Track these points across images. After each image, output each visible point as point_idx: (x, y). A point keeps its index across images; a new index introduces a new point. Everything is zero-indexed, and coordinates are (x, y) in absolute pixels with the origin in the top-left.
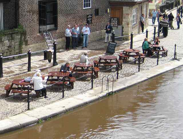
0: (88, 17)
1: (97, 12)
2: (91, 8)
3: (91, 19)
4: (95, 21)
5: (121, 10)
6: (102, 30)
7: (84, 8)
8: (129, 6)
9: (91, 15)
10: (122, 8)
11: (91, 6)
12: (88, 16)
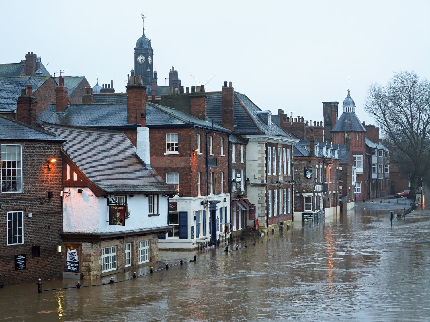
0: (17, 258)
2: (23, 245)
3: (24, 262)
5: (80, 247)
7: (8, 245)
8: (92, 243)
10: (81, 245)
11: (24, 241)
12: (17, 256)
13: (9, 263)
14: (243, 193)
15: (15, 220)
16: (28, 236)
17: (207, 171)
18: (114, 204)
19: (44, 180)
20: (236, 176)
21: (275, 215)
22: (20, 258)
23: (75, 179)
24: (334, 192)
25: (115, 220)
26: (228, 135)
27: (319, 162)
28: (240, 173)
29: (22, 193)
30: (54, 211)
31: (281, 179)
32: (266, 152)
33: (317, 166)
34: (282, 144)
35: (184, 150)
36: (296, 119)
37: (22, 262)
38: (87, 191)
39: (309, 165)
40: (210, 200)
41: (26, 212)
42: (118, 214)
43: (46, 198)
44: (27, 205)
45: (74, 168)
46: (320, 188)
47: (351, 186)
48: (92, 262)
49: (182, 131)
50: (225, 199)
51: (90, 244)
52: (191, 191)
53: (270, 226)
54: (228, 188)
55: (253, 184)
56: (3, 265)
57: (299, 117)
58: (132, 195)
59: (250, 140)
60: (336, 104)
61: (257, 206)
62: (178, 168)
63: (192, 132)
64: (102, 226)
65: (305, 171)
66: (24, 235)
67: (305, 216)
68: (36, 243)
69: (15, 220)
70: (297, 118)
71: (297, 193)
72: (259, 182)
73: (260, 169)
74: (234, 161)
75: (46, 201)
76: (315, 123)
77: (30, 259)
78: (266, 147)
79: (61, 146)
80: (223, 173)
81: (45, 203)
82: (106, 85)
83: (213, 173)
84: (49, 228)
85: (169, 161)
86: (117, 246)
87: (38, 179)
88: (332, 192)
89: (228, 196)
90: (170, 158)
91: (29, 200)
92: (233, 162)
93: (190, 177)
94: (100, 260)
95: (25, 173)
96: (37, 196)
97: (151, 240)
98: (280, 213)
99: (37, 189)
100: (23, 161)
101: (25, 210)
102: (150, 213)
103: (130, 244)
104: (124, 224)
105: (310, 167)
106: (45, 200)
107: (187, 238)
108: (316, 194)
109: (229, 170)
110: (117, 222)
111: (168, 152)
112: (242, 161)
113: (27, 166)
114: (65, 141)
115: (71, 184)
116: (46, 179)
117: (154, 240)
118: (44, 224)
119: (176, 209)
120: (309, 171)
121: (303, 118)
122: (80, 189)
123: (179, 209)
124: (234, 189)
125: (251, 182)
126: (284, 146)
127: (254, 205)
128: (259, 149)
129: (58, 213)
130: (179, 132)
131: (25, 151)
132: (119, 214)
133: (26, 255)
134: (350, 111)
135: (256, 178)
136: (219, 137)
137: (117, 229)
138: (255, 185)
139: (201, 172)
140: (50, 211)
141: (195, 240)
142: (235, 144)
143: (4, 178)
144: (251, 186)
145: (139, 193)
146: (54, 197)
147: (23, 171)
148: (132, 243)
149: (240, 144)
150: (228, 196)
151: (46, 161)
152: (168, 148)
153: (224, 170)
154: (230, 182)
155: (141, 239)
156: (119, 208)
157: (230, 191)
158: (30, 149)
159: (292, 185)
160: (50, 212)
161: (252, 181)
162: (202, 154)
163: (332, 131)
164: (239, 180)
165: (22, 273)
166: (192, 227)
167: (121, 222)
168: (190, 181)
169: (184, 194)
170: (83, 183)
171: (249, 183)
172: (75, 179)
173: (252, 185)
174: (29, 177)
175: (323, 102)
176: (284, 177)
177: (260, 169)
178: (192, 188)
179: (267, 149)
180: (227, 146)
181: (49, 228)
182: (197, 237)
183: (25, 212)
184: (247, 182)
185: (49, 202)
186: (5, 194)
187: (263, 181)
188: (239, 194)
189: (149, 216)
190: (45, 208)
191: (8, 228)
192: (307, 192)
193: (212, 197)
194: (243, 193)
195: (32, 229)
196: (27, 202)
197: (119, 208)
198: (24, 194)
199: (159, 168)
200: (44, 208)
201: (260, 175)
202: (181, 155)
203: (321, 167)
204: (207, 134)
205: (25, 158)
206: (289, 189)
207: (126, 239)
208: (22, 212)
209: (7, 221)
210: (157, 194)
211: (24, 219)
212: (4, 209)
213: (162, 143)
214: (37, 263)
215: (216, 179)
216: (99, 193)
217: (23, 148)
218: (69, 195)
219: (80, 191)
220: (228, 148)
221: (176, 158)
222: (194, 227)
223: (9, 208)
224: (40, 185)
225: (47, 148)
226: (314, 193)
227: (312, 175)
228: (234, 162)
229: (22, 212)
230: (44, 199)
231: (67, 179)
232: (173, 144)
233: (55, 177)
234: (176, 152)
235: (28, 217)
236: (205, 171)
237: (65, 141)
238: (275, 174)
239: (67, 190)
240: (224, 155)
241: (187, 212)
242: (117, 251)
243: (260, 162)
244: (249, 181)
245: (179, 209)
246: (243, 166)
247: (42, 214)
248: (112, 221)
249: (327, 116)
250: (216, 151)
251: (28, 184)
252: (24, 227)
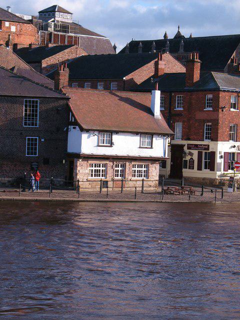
15: (32, 143)
38: (77, 127)
45: (73, 115)
58: (117, 132)
69: (32, 143)
84: (57, 148)
115: (72, 124)
183: (39, 138)
202: (213, 111)
219: (74, 128)
230: (53, 131)
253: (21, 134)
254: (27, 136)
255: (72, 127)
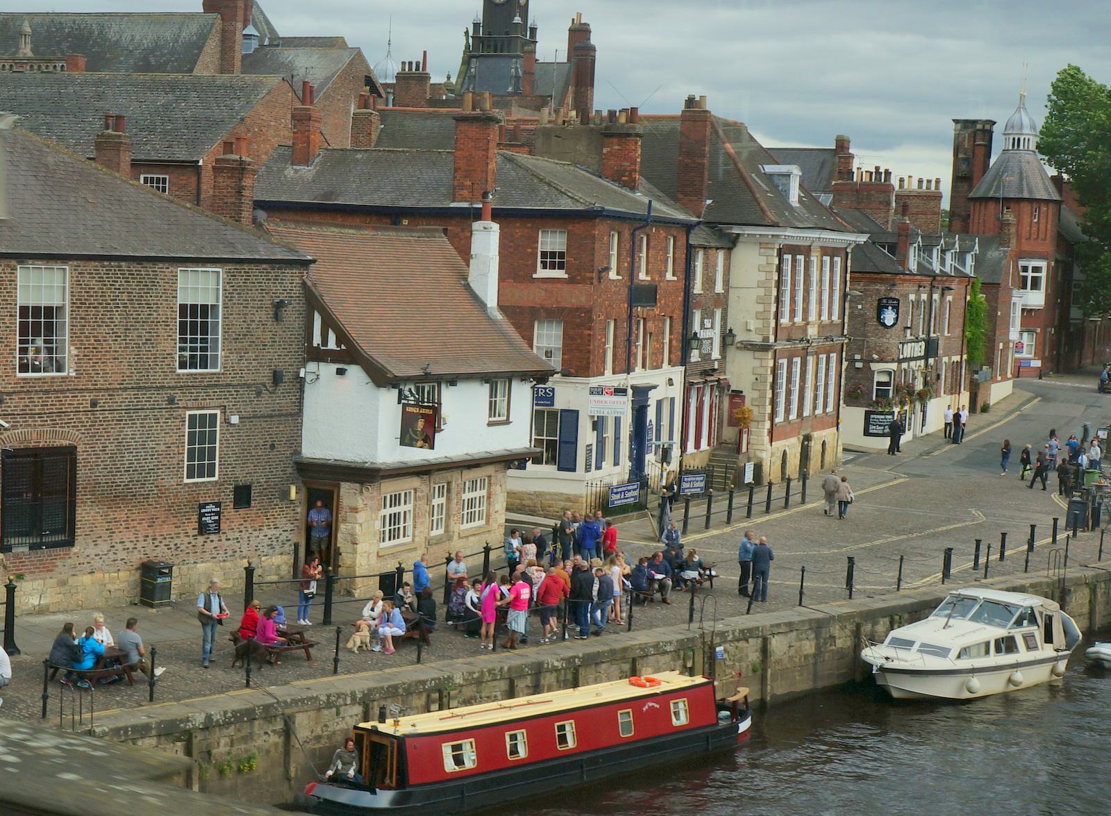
0: (203, 511)
1: (243, 496)
2: (216, 482)
3: (217, 518)
4: (235, 525)
6: (263, 558)
7: (186, 481)
8: (362, 483)
9: (218, 505)
13: (186, 519)
14: (716, 363)
15: (202, 430)
16: (228, 464)
17: (630, 317)
18: (412, 403)
19: (266, 345)
20: (702, 324)
21: (793, 416)
22: (209, 510)
23: (332, 345)
24: (956, 358)
25: (414, 436)
26: (688, 228)
27: (920, 286)
28: (711, 316)
29: (219, 374)
30: (284, 412)
31: (812, 332)
32: (779, 269)
33: (912, 297)
34: (821, 247)
35: (577, 269)
36: (871, 173)
37: (213, 518)
38: (355, 372)
39: (892, 295)
40: (635, 382)
41: (225, 413)
42: (421, 424)
43: (269, 382)
44: (228, 398)
46: (919, 349)
47: (1007, 343)
48: (361, 525)
49: (577, 225)
50: (670, 380)
51: (358, 485)
52: (589, 363)
53: (779, 445)
54: (679, 353)
55: (741, 342)
56: (174, 524)
57: (877, 168)
58: (453, 380)
59: (741, 239)
60: (987, 127)
61: (749, 395)
62: (564, 309)
63: (600, 228)
64: (387, 450)
65: (881, 308)
66: (220, 461)
67: (872, 416)
68: (242, 480)
69: (202, 430)
70: (874, 170)
71: (857, 361)
72: (757, 339)
73: (760, 308)
74: (698, 289)
75: (267, 390)
76: (920, 181)
77: (229, 511)
78: (780, 254)
79: (305, 272)
80: (671, 318)
81: (265, 395)
82: (410, 63)
83: (644, 319)
84: (272, 447)
85: (543, 293)
86: (415, 490)
87: (254, 342)
88: (950, 359)
89: (677, 373)
90: (545, 286)
91: (234, 386)
92: (695, 292)
93: (589, 332)
94: (377, 519)
95: (226, 330)
96: (249, 379)
97: (490, 477)
98: (806, 413)
99: (251, 363)
100: (224, 304)
101: (224, 409)
102: (493, 419)
103: (443, 486)
104: (432, 447)
105: (894, 299)
106: (266, 387)
107: (574, 470)
108: (904, 365)
109: (684, 311)
110: (417, 441)
111: (541, 273)
112: (719, 288)
113: (231, 314)
114: (314, 261)
115: (319, 355)
116: (271, 343)
117: (496, 477)
118: (261, 439)
119: (552, 404)
120: (890, 308)
121: (888, 173)
122: (340, 366)
123: (559, 404)
124: (695, 356)
125: (738, 339)
126: (826, 251)
127: (741, 392)
128: (763, 260)
129: (291, 415)
130: (570, 228)
131: (228, 283)
132: (422, 424)
133: (222, 505)
134: (1021, 147)
135: (750, 330)
136: (664, 235)
137: (417, 455)
138: (749, 347)
139: (615, 320)
140: (275, 410)
141: (594, 474)
142: (705, 248)
143: (183, 340)
144: (738, 348)
145: (469, 377)
146: (286, 382)
147: (223, 325)
148: (449, 483)
149: (717, 249)
150: (677, 373)
151: (271, 304)
152: (542, 262)
153: (673, 312)
154: (687, 341)
155: (469, 475)
156: (423, 411)
157: (684, 361)
158: (239, 278)
159: (843, 345)
160: (277, 413)
161: (740, 336)
162: (620, 278)
163: (971, 195)
164: (708, 334)
165: (212, 541)
166: (588, 446)
167: (425, 441)
168: (589, 341)
169: (572, 370)
170: (349, 355)
171: (733, 341)
172: (332, 345)
173: (739, 345)
174: (234, 339)
175: (956, 121)
176: (822, 327)
177: (760, 308)
178: (591, 357)
179: (781, 261)
180: (684, 256)
181: (272, 447)
182: (598, 467)
184: (729, 340)
185: (274, 393)
186: (183, 375)
187: (766, 339)
188: (708, 367)
189: (490, 424)
190: (267, 404)
191: (186, 447)
192: (881, 360)
193: (639, 377)
194: (716, 363)
195: (237, 449)
196: (228, 392)
197: (423, 411)
198: (223, 374)
199: (519, 307)
200: (266, 404)
201: (759, 324)
202: (571, 281)
203: (924, 297)
204: (635, 230)
205: (227, 297)
206: (834, 356)
207: (436, 477)
208: (218, 412)
209: (187, 430)
210: (509, 377)
211: (220, 427)
212: (181, 406)
213: (530, 250)
214: (245, 521)
215: (651, 334)
216: (380, 378)
217: (225, 276)
218: (318, 378)
219: (341, 372)
220: (686, 259)
221: (559, 285)
222: (591, 445)
223: (190, 404)
224: (256, 356)
225: (276, 276)
226: (900, 361)
227: (897, 319)
228: (700, 292)
229: (218, 412)
230: (264, 385)
231: (315, 345)
232: (553, 254)
233: (289, 338)
234: (560, 274)
235: (229, 423)
236: (625, 316)
237: (314, 261)
238: (798, 319)
239: (312, 366)
240: (673, 275)
241: (577, 412)
242: (415, 499)
243: (761, 292)
244: (734, 336)
245: (559, 404)
246: (722, 302)
247: (259, 417)
248: (406, 439)
249: (961, 156)
250: (656, 268)
251: (232, 353)
252: (220, 444)
253: (171, 401)
254: (187, 408)
255: (333, 367)
